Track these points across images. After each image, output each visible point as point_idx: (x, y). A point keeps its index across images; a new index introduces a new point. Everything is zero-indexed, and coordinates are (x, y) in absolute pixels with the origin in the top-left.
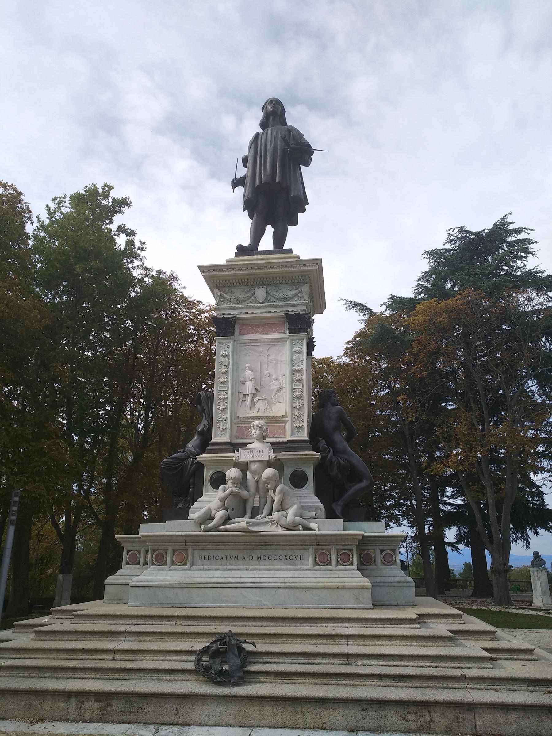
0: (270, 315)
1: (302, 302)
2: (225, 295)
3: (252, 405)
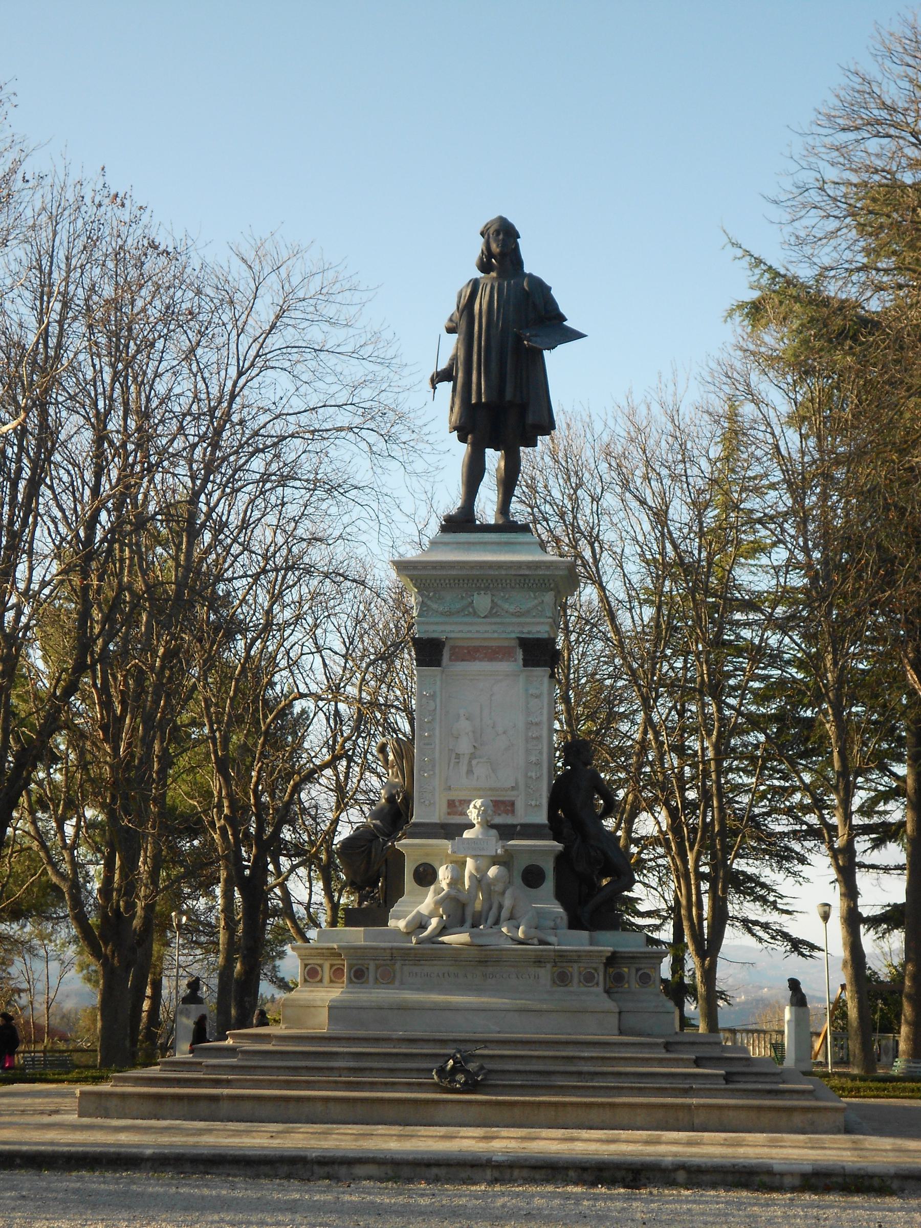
0: (496, 635)
1: (542, 620)
2: (429, 603)
3: (470, 772)
